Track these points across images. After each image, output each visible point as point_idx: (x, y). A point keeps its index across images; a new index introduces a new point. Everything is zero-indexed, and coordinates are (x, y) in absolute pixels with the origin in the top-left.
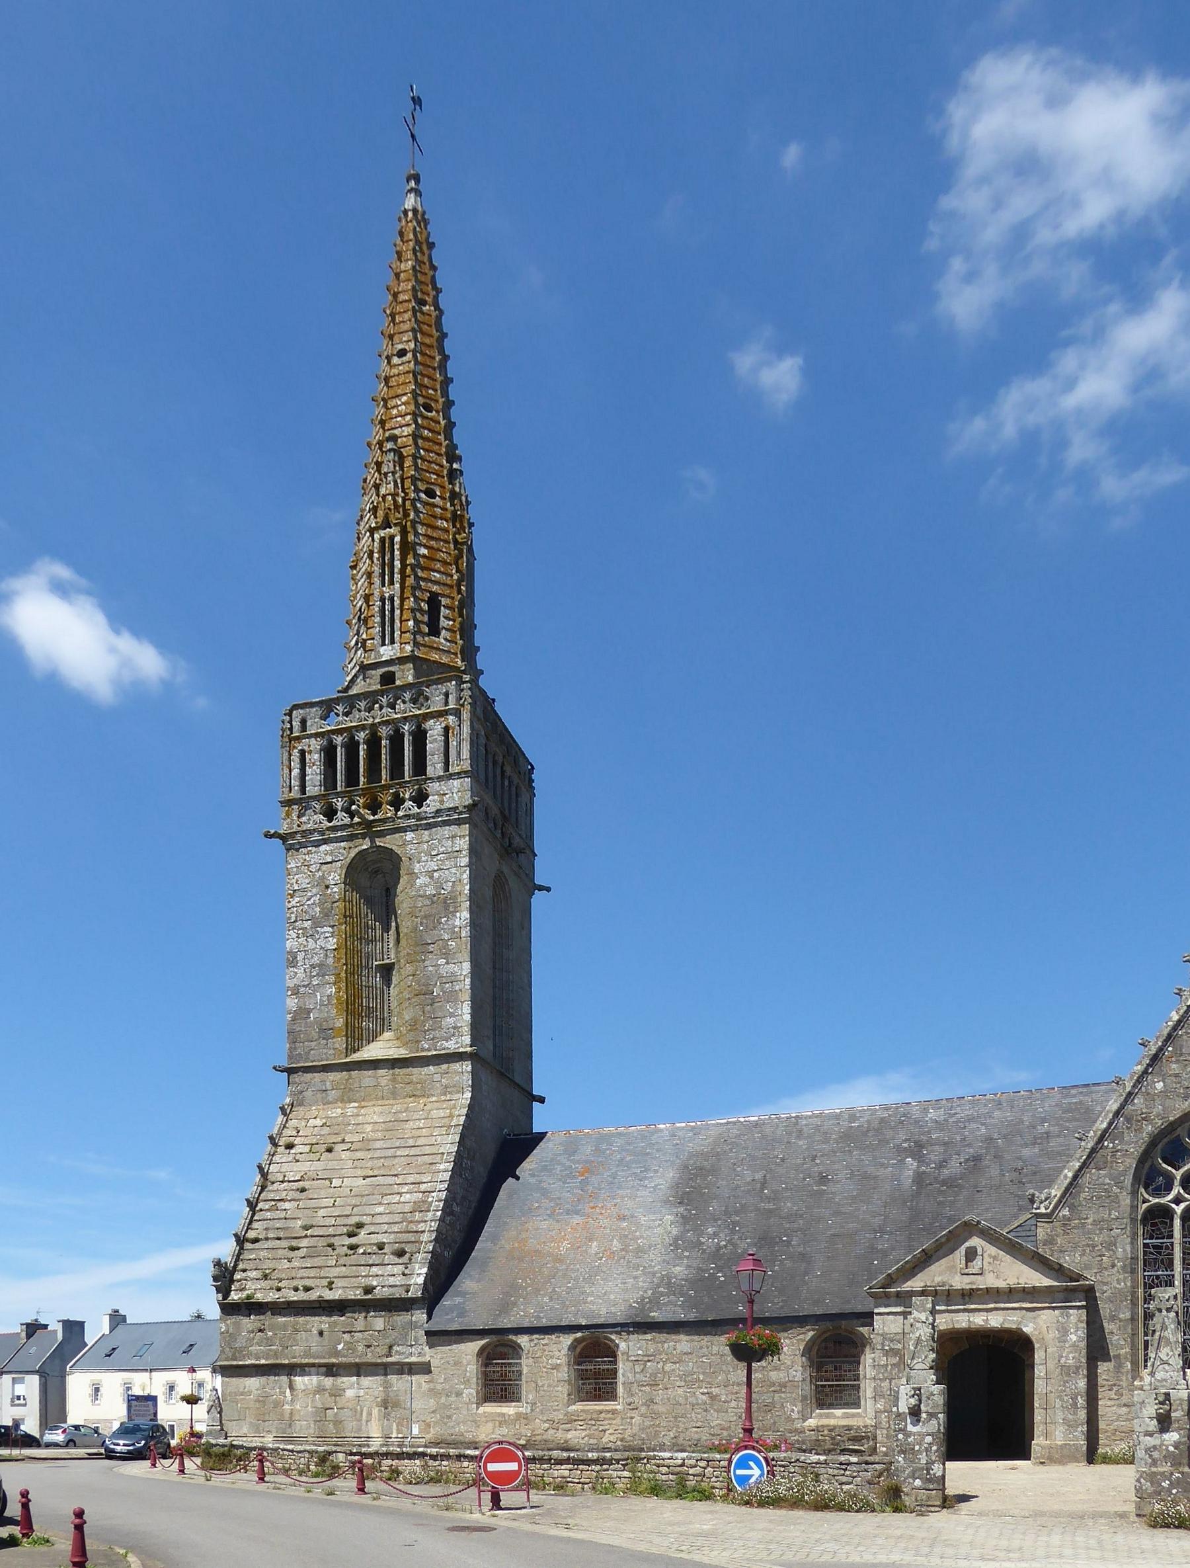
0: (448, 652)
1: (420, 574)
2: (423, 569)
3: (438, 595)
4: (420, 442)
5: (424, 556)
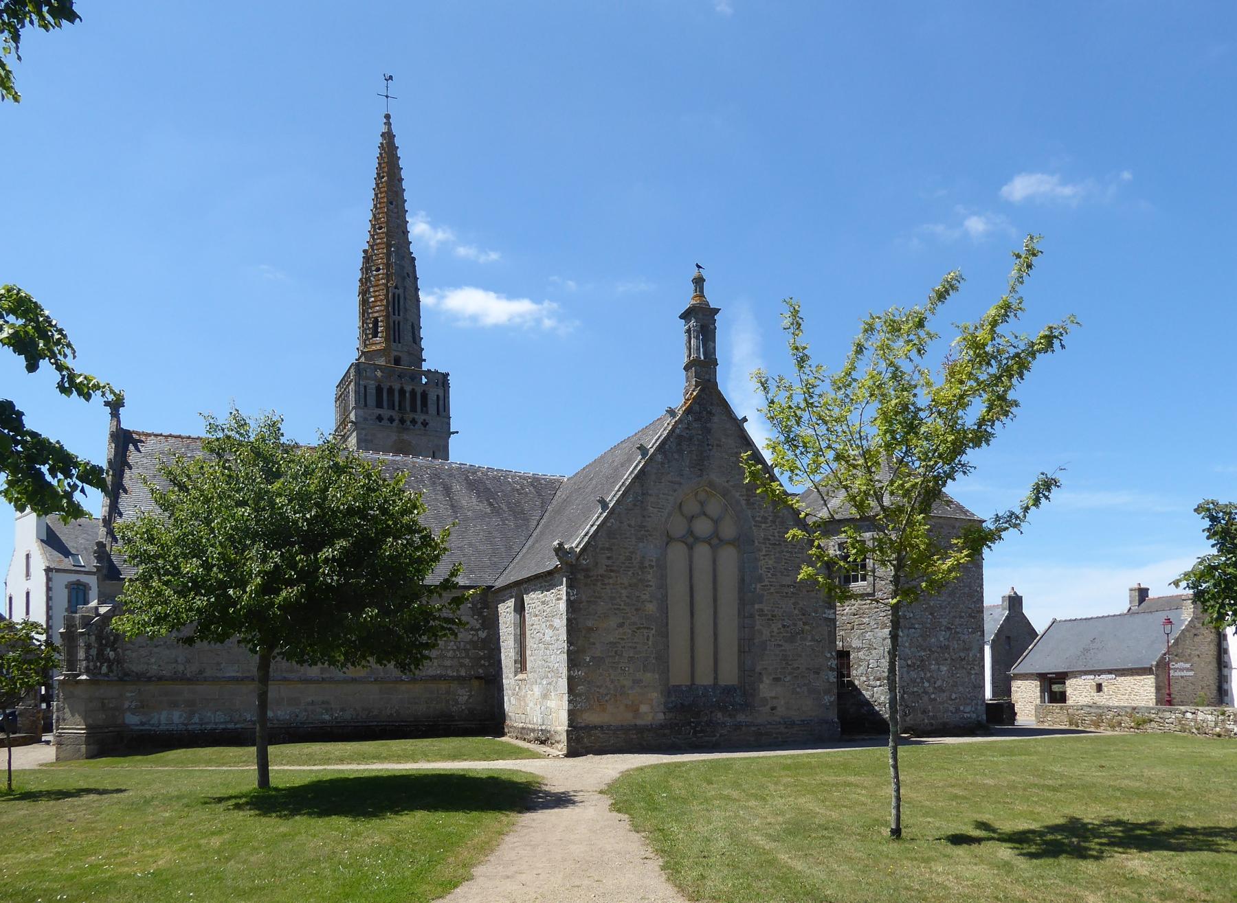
0: (380, 343)
1: (370, 311)
2: (371, 308)
3: (378, 317)
4: (375, 247)
5: (373, 302)
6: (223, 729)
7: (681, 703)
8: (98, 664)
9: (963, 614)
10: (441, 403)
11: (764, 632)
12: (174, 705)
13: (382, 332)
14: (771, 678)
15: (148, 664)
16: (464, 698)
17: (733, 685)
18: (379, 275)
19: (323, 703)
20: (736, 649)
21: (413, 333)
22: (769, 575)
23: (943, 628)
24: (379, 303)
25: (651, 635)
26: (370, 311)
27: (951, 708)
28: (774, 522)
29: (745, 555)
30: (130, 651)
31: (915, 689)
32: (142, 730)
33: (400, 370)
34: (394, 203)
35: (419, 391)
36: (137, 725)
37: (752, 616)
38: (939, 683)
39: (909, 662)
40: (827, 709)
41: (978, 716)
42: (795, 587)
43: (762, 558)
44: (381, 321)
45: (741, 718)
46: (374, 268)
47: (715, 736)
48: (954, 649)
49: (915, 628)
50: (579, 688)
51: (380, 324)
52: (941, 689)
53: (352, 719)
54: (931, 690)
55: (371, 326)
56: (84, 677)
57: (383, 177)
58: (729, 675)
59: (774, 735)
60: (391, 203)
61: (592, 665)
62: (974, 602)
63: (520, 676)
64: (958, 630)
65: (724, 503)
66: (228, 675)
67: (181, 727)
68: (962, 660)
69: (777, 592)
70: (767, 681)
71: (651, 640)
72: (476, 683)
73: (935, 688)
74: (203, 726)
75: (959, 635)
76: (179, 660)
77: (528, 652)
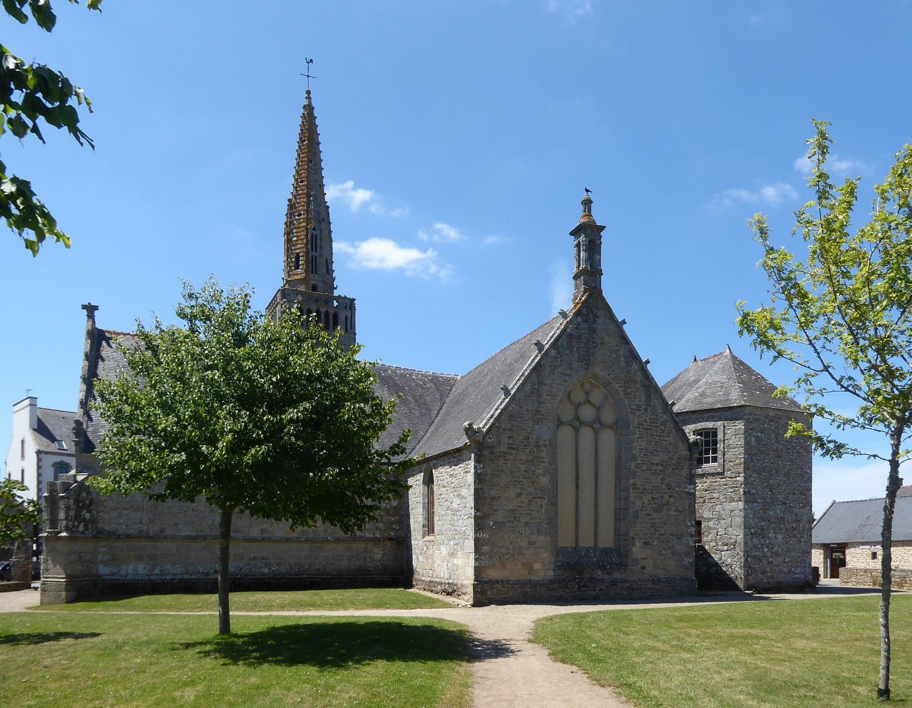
1: (293, 248)
4: (298, 197)
6: (180, 579)
7: (568, 563)
8: (76, 523)
9: (796, 491)
10: (349, 322)
11: (637, 503)
12: (140, 559)
13: (302, 265)
14: (642, 542)
15: (118, 524)
16: (378, 555)
17: (610, 548)
18: (300, 219)
19: (263, 558)
20: (613, 517)
21: (327, 266)
22: (642, 455)
23: (779, 503)
24: (300, 242)
25: (544, 504)
26: (293, 248)
27: (784, 570)
28: (646, 410)
29: (622, 438)
30: (102, 513)
31: (757, 554)
32: (112, 580)
33: (316, 295)
34: (313, 162)
35: (331, 312)
36: (108, 575)
37: (627, 489)
38: (775, 549)
39: (752, 531)
40: (687, 568)
41: (805, 577)
42: (662, 465)
43: (636, 440)
44: (302, 256)
45: (617, 575)
46: (296, 214)
47: (595, 590)
48: (788, 521)
49: (758, 503)
50: (484, 548)
51: (301, 258)
52: (777, 554)
53: (286, 572)
54: (769, 554)
55: (293, 260)
56: (64, 534)
57: (305, 141)
58: (607, 539)
59: (644, 591)
60: (311, 162)
61: (495, 529)
62: (805, 482)
63: (427, 538)
64: (791, 505)
65: (605, 393)
66: (184, 534)
67: (144, 577)
68: (794, 529)
69: (647, 470)
70: (638, 544)
71: (544, 508)
72: (388, 544)
73: (772, 553)
74: (164, 577)
75: (792, 509)
76: (144, 521)
77: (436, 518)
